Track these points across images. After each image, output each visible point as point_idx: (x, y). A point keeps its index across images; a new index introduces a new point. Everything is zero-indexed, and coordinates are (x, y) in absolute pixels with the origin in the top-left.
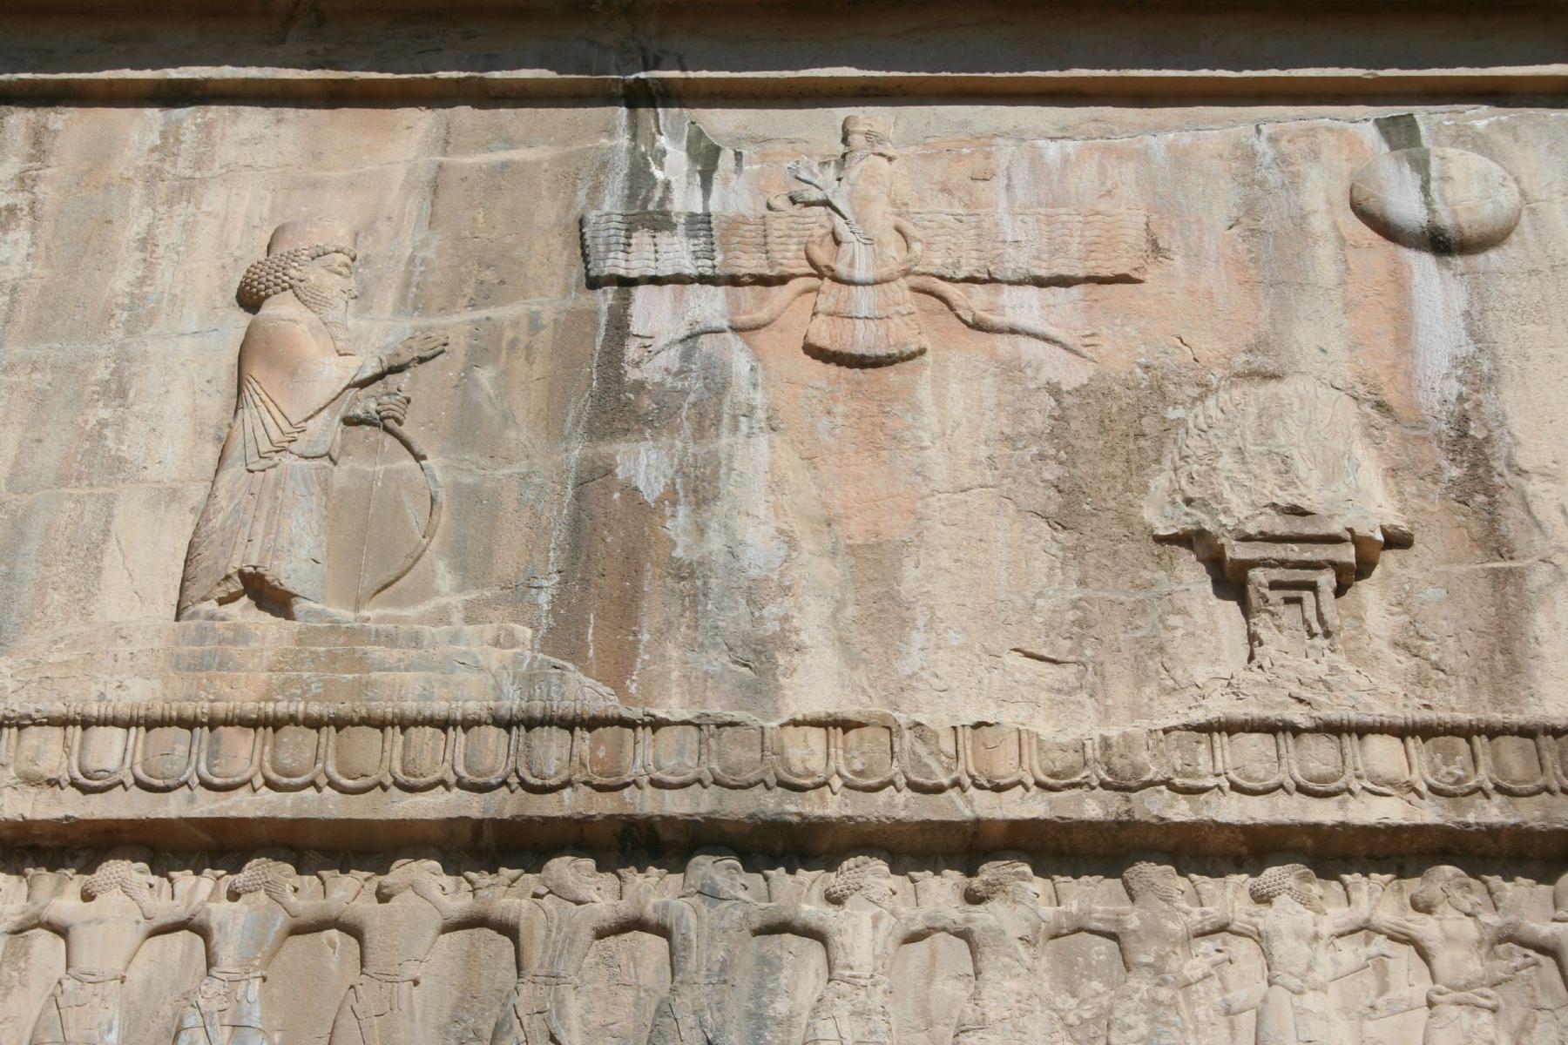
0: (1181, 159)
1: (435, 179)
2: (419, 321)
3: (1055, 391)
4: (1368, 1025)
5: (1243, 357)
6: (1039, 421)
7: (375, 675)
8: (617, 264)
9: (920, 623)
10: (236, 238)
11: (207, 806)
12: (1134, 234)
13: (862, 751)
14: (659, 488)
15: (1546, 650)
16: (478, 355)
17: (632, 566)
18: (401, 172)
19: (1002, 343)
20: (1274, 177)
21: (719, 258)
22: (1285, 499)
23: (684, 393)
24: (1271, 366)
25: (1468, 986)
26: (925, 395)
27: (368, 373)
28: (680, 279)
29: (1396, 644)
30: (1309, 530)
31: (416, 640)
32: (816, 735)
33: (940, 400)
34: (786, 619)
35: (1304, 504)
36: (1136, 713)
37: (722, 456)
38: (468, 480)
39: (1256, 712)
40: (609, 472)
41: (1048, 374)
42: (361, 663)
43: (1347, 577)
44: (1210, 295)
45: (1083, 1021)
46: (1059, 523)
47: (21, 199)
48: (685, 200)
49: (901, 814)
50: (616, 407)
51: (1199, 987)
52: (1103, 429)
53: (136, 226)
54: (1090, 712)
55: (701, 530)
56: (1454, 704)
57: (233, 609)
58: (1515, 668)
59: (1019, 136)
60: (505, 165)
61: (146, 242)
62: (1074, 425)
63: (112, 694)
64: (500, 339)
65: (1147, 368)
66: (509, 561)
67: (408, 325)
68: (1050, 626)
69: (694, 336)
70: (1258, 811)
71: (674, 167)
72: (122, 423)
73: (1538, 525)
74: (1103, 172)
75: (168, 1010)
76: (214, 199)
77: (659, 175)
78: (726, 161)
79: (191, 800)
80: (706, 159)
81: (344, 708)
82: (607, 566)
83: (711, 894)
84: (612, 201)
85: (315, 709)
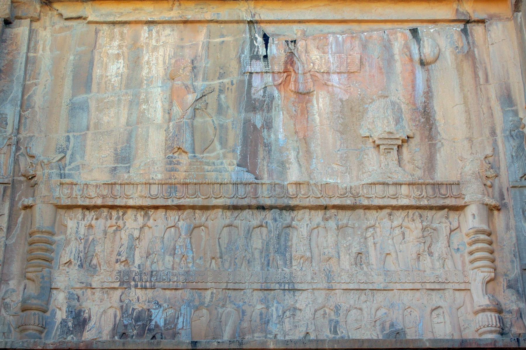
1: (208, 46)
2: (207, 83)
3: (341, 100)
4: (401, 246)
5: (380, 92)
6: (339, 109)
7: (206, 173)
8: (249, 69)
9: (315, 157)
10: (167, 61)
11: (176, 202)
12: (357, 61)
15: (438, 162)
16: (221, 91)
17: (256, 146)
18: (201, 43)
21: (270, 67)
22: (387, 130)
23: (265, 101)
24: (386, 95)
25: (420, 238)
26: (315, 102)
27: (198, 97)
29: (409, 162)
30: (392, 137)
31: (214, 163)
33: (318, 104)
34: (288, 156)
35: (391, 131)
37: (273, 117)
38: (221, 123)
39: (381, 180)
40: (250, 121)
41: (340, 96)
42: (203, 170)
44: (374, 76)
45: (347, 246)
46: (342, 133)
51: (369, 239)
54: (348, 178)
55: (269, 136)
57: (176, 155)
58: (432, 166)
59: (334, 33)
60: (223, 42)
61: (148, 62)
62: (346, 109)
63: (155, 178)
64: (225, 87)
65: (360, 95)
66: (231, 142)
68: (341, 157)
69: (266, 87)
70: (381, 202)
73: (439, 133)
74: (351, 43)
75: (172, 244)
76: (161, 52)
77: (256, 45)
78: (270, 40)
79: (173, 201)
80: (266, 38)
83: (275, 220)
84: (247, 51)
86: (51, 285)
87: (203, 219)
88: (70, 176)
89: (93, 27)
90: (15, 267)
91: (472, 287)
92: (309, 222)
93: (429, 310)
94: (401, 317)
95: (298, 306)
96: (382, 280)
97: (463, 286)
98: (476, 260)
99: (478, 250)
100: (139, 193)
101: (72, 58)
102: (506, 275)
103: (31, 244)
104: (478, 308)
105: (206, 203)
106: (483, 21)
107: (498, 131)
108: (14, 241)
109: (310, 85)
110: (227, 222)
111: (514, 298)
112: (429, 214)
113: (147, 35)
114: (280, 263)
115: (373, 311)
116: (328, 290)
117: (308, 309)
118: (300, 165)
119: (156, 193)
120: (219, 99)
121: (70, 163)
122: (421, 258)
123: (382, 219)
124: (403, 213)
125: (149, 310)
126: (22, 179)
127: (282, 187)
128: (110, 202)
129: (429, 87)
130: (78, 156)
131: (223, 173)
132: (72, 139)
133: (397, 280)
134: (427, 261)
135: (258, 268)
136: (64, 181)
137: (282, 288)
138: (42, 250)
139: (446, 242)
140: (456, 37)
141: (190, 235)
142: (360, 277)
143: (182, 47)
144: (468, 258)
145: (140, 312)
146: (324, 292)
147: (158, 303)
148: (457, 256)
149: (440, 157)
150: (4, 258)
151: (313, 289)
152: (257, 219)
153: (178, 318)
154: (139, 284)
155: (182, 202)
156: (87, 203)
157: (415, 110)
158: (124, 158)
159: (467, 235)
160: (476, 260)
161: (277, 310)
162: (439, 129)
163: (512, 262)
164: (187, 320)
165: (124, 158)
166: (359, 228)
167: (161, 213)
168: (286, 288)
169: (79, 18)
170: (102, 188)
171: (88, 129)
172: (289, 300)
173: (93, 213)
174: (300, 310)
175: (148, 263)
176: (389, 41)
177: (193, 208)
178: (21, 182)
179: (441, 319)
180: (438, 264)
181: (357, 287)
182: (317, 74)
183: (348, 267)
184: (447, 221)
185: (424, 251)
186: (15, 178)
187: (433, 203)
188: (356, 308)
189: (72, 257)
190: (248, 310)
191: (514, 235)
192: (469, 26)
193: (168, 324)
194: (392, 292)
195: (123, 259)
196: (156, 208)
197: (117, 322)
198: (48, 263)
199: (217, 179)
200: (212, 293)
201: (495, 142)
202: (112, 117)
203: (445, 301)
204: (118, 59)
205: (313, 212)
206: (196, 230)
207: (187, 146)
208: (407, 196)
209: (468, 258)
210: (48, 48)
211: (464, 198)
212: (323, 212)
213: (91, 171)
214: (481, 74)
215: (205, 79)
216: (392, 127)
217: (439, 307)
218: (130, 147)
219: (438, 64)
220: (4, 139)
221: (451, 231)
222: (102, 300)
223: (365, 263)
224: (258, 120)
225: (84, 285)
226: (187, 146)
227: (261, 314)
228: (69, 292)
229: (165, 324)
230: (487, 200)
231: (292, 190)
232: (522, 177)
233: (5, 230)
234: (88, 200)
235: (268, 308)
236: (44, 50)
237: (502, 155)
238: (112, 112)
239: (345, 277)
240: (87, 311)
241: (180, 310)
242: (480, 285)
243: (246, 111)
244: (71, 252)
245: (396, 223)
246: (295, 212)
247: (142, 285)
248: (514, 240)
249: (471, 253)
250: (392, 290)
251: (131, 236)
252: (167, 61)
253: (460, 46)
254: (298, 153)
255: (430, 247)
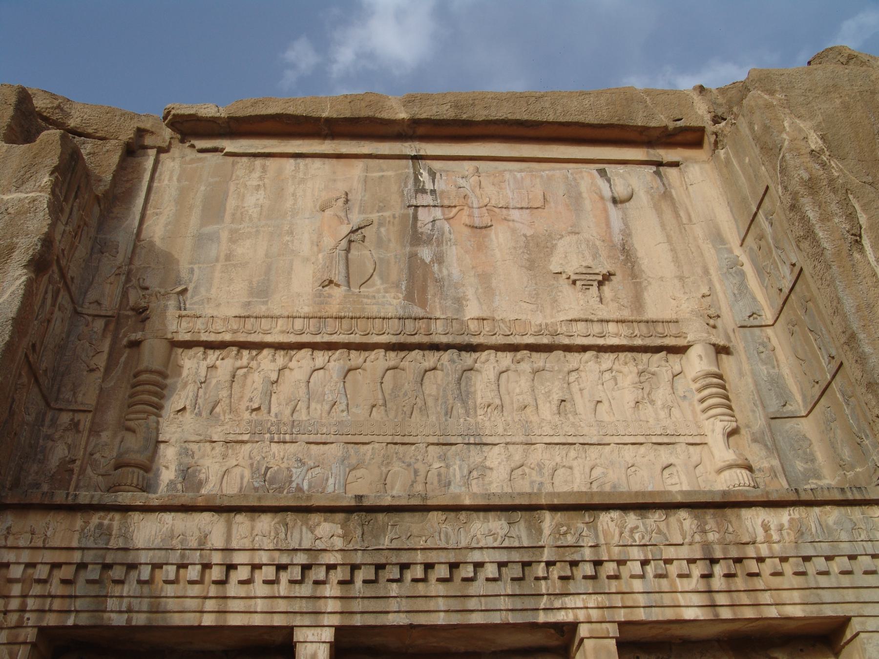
0: (549, 178)
3: (525, 236)
6: (522, 244)
8: (413, 202)
11: (327, 338)
12: (541, 197)
13: (487, 327)
14: (429, 259)
17: (425, 280)
19: (511, 224)
20: (573, 183)
21: (439, 201)
22: (584, 264)
26: (493, 236)
28: (428, 206)
31: (374, 297)
32: (476, 321)
36: (552, 317)
39: (583, 317)
43: (601, 284)
46: (530, 269)
47: (261, 183)
48: (429, 186)
49: (499, 342)
50: (416, 238)
52: (538, 245)
53: (291, 190)
55: (440, 271)
56: (626, 314)
58: (641, 306)
59: (511, 171)
61: (294, 195)
66: (394, 276)
67: (362, 216)
71: (425, 177)
72: (292, 241)
78: (438, 175)
80: (432, 174)
81: (358, 315)
82: (418, 281)
83: (452, 361)
85: (351, 314)
86: (157, 437)
87: (361, 360)
88: (191, 309)
89: (231, 159)
90: (111, 416)
91: (709, 440)
92: (496, 365)
93: (659, 468)
94: (624, 476)
95: (488, 463)
96: (595, 433)
97: (697, 440)
98: (710, 407)
99: (711, 396)
100: (279, 328)
101: (203, 188)
102: (748, 426)
103: (134, 386)
104: (722, 464)
105: (365, 340)
106: (676, 164)
107: (712, 271)
108: (112, 384)
109: (486, 220)
110: (392, 363)
111: (763, 453)
112: (645, 357)
113: (293, 168)
114: (462, 411)
115: (587, 470)
116: (527, 444)
117: (502, 467)
118: (480, 303)
119: (300, 328)
120: (378, 233)
121: (192, 297)
122: (641, 406)
123: (587, 362)
124: (612, 356)
125: (288, 469)
126: (130, 313)
127: (462, 323)
128: (242, 338)
129: (626, 224)
130: (203, 290)
131: (387, 306)
132: (196, 271)
133: (615, 432)
134: (647, 411)
135: (433, 418)
136: (183, 313)
137: (466, 441)
138: (150, 393)
139: (669, 388)
140: (649, 178)
141: (344, 378)
142: (566, 429)
143: (335, 180)
144: (700, 407)
145: (276, 472)
146: (521, 448)
147: (301, 461)
148: (685, 404)
149: (649, 297)
150: (98, 403)
151: (507, 444)
152: (429, 361)
153: (327, 480)
154: (276, 436)
155: (335, 338)
156: (212, 338)
157: (613, 247)
158: (262, 291)
159: (695, 380)
160: (710, 407)
161: (460, 468)
162: (643, 267)
163: (754, 411)
164: (340, 482)
165: (262, 291)
166: (559, 371)
167: (305, 353)
168: (472, 441)
169: (215, 150)
170: (232, 321)
171: (217, 260)
172: (475, 456)
173: (218, 352)
174: (491, 469)
175: (288, 412)
176: (575, 179)
177: (349, 346)
178: (128, 317)
179: (675, 480)
180: (663, 414)
181: (564, 441)
182: (495, 209)
183: (549, 417)
184: (667, 364)
185: (643, 398)
186: (122, 312)
187: (648, 342)
188: (564, 466)
189: (188, 403)
190: (422, 469)
191: (750, 380)
192: (661, 168)
193: (314, 487)
194: (607, 447)
195: (256, 406)
196: (300, 346)
197: (245, 484)
198: (155, 410)
199: (379, 312)
200: (373, 449)
201: (710, 281)
202: (248, 249)
203: (677, 458)
204: (257, 190)
205: (499, 353)
206: (351, 373)
207: (339, 278)
208: (617, 335)
209: (700, 407)
210: (175, 178)
211: (686, 338)
212: (512, 354)
213: (218, 305)
214: (682, 214)
215: (362, 211)
216: (589, 262)
217: (671, 465)
218: (268, 280)
219: (632, 202)
220: (112, 267)
221: (674, 376)
222: (225, 456)
223: (570, 412)
224: (426, 253)
225: (202, 438)
226: (339, 278)
227: (439, 475)
228: (181, 447)
229: (310, 487)
230: (714, 340)
231: (473, 326)
232: (750, 316)
233: (102, 370)
234: (213, 335)
235: (448, 466)
236: (170, 179)
237: (721, 295)
238: (248, 243)
239: (547, 430)
240: (204, 471)
241: (331, 469)
242: (721, 436)
243: (412, 245)
244: (187, 397)
245: (605, 366)
246: (478, 354)
247: (279, 438)
248: (751, 386)
249: (702, 401)
250: (609, 444)
251: (266, 379)
252: (316, 194)
253: (655, 186)
254: (477, 289)
255: (649, 394)
